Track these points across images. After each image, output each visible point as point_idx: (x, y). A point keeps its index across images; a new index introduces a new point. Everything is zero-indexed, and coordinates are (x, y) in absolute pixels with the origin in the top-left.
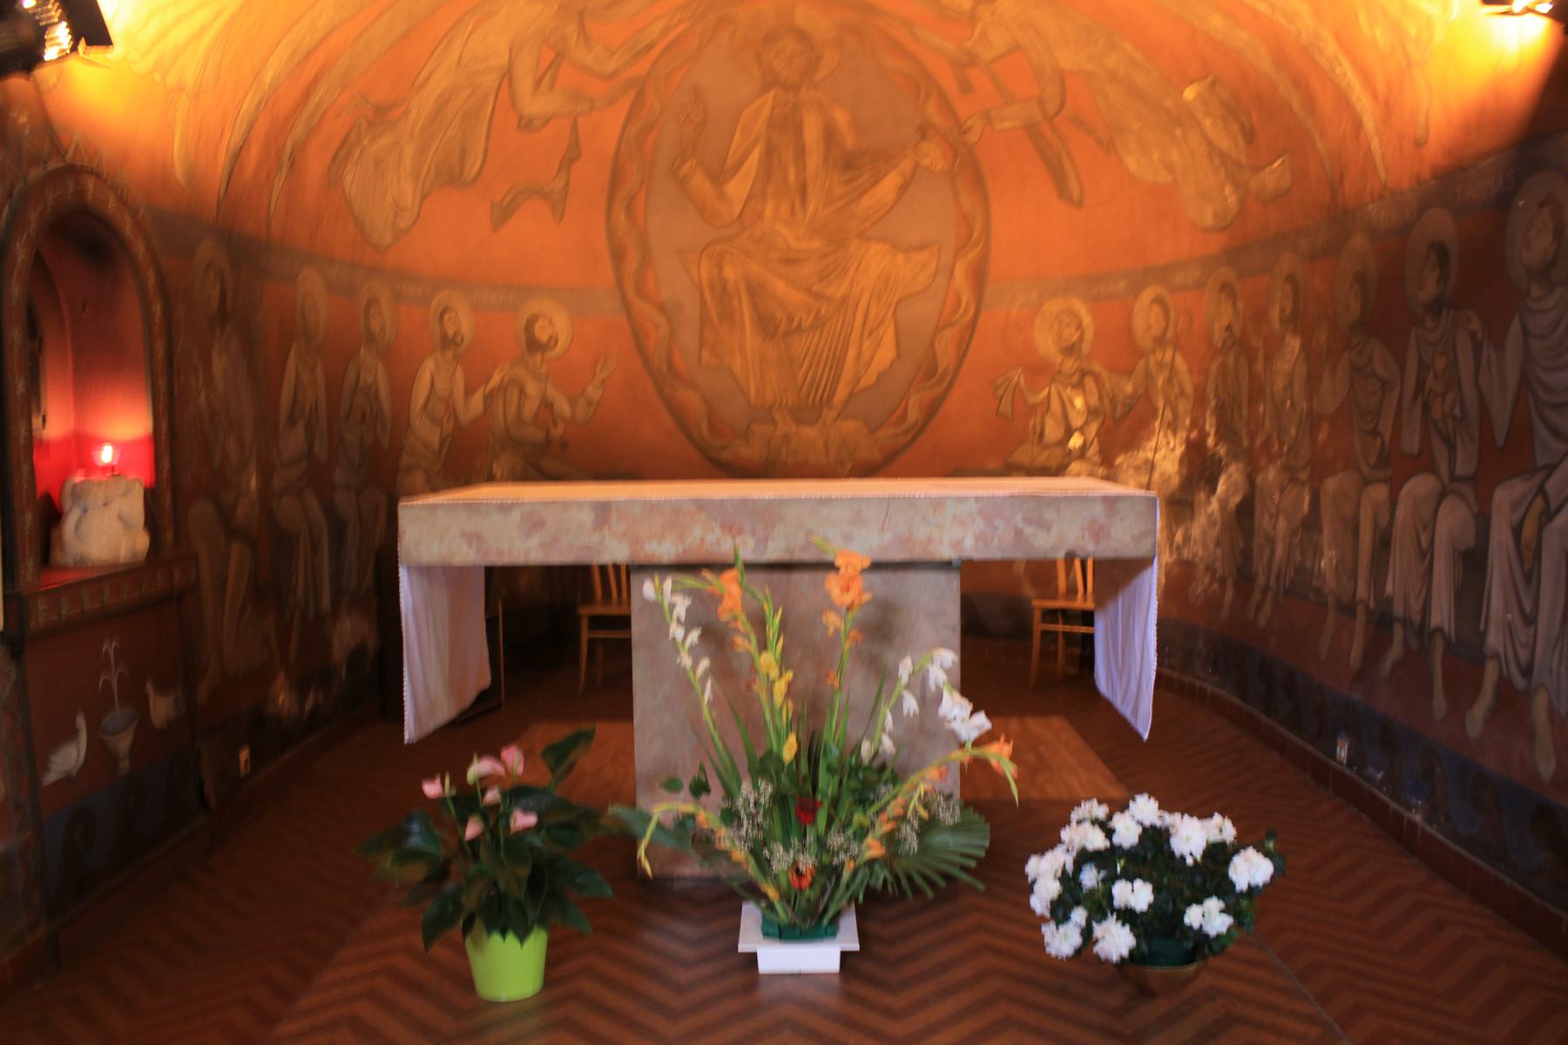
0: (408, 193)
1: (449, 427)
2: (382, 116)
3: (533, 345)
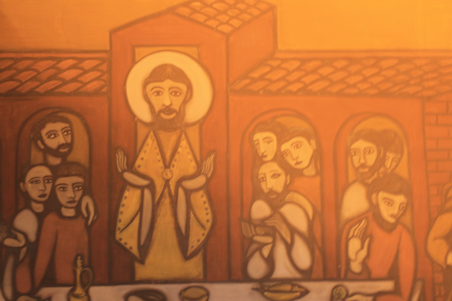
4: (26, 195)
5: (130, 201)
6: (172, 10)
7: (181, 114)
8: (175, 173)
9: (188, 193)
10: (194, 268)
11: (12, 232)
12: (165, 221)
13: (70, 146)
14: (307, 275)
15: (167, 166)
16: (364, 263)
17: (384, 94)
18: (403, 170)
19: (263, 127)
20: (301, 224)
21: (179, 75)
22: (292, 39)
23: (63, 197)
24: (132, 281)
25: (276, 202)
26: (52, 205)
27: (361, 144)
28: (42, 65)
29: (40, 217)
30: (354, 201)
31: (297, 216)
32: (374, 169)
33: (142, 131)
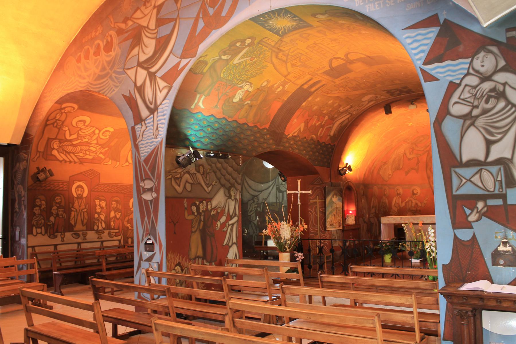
0: (390, 172)
1: (398, 208)
2: (385, 163)
3: (414, 194)
4: (52, 213)
5: (73, 214)
6: (81, 173)
7: (82, 195)
8: (81, 208)
9: (83, 212)
10: (84, 228)
11: (49, 221)
12: (79, 218)
13: (61, 202)
14: (104, 229)
15: (80, 207)
16: (114, 227)
17: (118, 192)
18: (120, 208)
19: (96, 199)
20: (103, 219)
21: (82, 187)
22: (102, 181)
23: (60, 213)
24: (73, 231)
25: (99, 214)
26: (57, 215)
27: (114, 203)
28: (56, 184)
29: (55, 218)
30: (112, 214)
31: (103, 217)
32: (116, 208)
33: (75, 199)
